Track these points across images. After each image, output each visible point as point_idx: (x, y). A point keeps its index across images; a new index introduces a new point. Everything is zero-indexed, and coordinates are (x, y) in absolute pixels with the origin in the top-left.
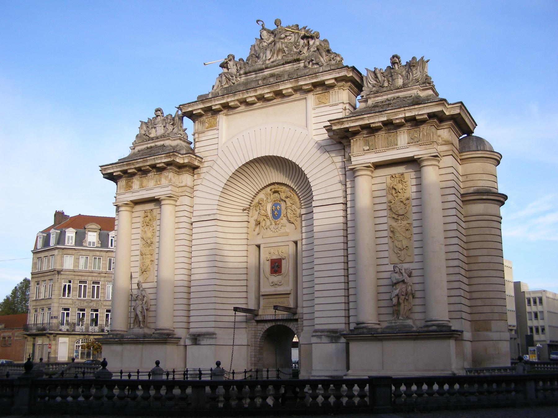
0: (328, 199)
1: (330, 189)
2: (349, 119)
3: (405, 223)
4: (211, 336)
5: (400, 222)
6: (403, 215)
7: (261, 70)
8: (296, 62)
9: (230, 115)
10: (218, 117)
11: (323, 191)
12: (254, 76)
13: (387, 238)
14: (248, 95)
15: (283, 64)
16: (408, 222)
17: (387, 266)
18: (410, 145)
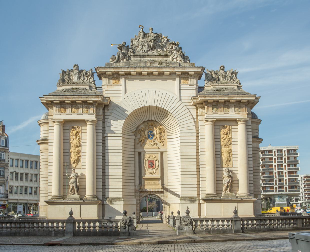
0: (189, 133)
1: (189, 128)
2: (209, 96)
3: (229, 148)
4: (120, 200)
5: (226, 148)
6: (228, 145)
7: (144, 56)
8: (165, 56)
9: (129, 79)
10: (121, 78)
11: (185, 129)
12: (139, 58)
13: (220, 155)
14: (144, 70)
15: (158, 56)
16: (231, 148)
17: (220, 168)
18: (236, 113)
